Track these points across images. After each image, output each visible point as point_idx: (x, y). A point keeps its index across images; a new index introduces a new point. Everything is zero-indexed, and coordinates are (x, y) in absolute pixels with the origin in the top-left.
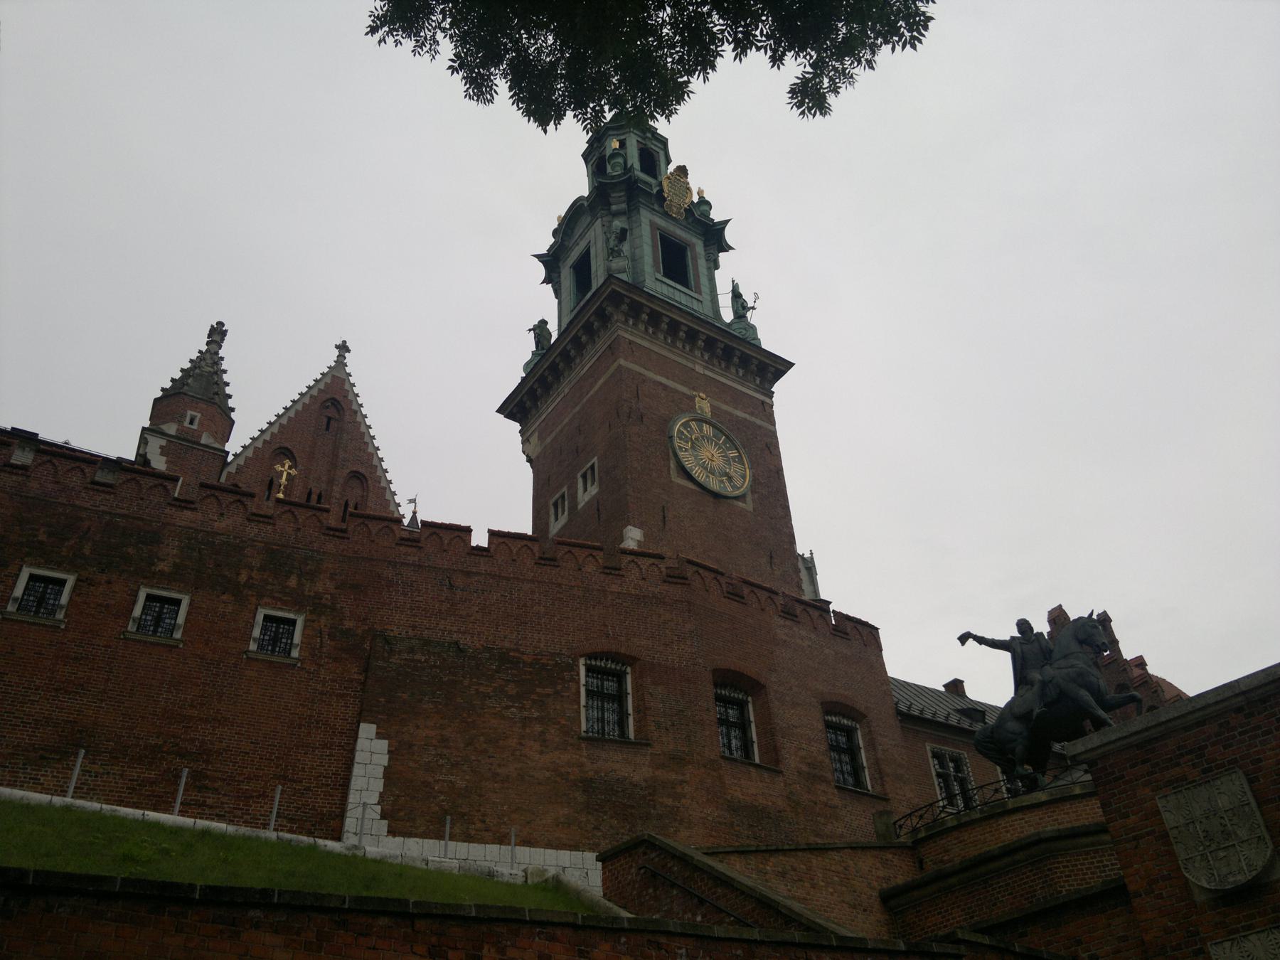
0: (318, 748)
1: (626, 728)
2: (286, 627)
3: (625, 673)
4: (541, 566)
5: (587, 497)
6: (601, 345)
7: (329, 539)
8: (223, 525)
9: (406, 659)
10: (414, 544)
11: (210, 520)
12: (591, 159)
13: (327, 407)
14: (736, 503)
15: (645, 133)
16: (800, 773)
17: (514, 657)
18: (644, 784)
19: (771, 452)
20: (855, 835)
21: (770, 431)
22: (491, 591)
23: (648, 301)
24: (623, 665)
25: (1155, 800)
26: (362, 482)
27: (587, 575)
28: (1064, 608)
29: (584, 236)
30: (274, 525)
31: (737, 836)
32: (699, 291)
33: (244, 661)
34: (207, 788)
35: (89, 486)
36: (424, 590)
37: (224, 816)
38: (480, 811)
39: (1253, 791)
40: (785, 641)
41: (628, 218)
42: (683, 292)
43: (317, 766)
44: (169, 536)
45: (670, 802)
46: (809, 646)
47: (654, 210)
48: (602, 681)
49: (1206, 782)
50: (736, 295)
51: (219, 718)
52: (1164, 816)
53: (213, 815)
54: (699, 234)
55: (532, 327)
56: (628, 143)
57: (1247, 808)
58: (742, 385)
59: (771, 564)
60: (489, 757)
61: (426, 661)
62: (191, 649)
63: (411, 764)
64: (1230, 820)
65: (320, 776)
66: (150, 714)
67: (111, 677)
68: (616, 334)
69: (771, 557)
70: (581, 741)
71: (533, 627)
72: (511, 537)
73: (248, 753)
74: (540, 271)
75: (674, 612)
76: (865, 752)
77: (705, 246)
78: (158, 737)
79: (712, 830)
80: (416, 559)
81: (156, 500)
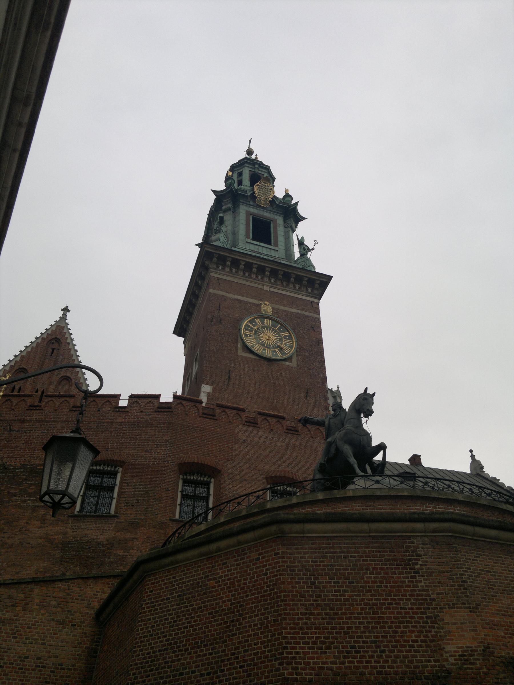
13: (53, 343)
14: (284, 363)
18: (105, 542)
19: (314, 330)
21: (316, 318)
23: (229, 254)
26: (69, 381)
32: (276, 245)
40: (244, 440)
41: (233, 212)
45: (121, 553)
46: (264, 442)
47: (250, 205)
50: (301, 243)
54: (280, 214)
59: (307, 397)
69: (307, 393)
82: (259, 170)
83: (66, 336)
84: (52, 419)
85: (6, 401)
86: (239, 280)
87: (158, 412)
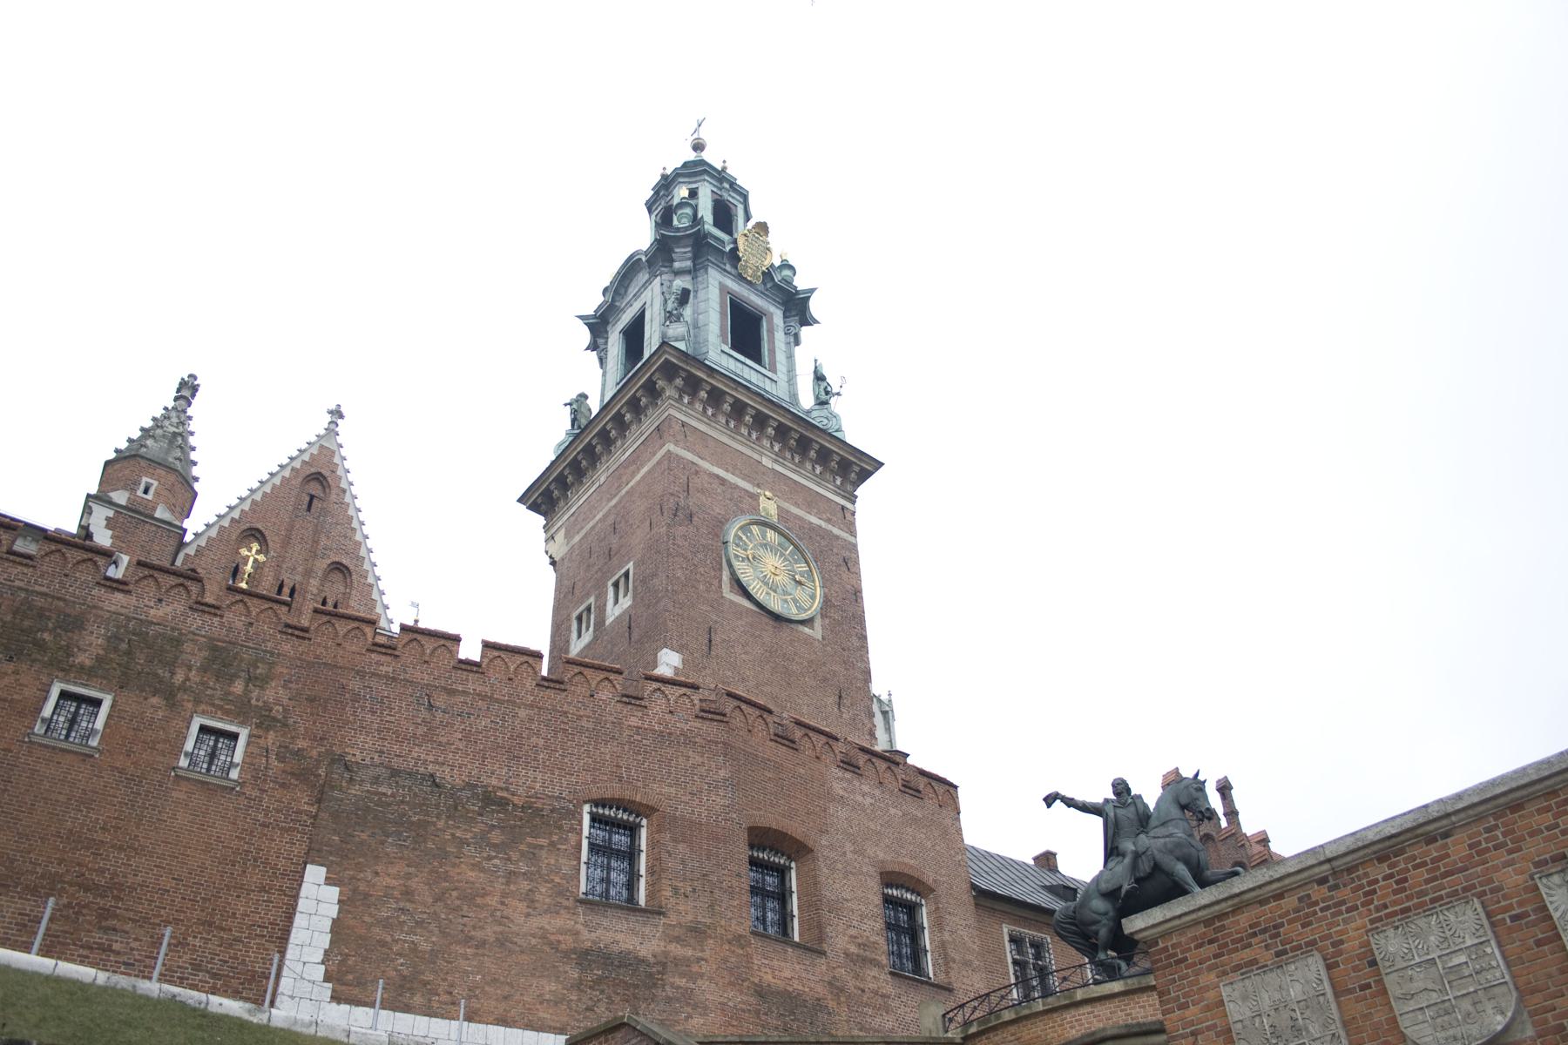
0: (254, 891)
1: (635, 893)
2: (226, 741)
3: (639, 826)
4: (544, 689)
5: (618, 611)
6: (649, 424)
7: (287, 639)
8: (160, 613)
9: (368, 791)
10: (390, 651)
11: (145, 606)
12: (656, 209)
15: (721, 183)
16: (847, 954)
17: (502, 798)
18: (652, 960)
20: (908, 1030)
21: (850, 543)
22: (478, 716)
23: (709, 376)
24: (637, 816)
25: (1219, 987)
26: (344, 575)
27: (601, 703)
28: (1180, 771)
29: (639, 296)
30: (221, 616)
31: (763, 1026)
32: (773, 369)
33: (171, 778)
34: (114, 930)
35: (5, 556)
36: (397, 708)
37: (134, 965)
38: (447, 980)
39: (1331, 979)
41: (693, 279)
42: (754, 369)
43: (252, 912)
44: (94, 622)
45: (682, 982)
46: (871, 804)
48: (610, 833)
49: (1278, 967)
50: (819, 378)
51: (136, 846)
52: (1227, 1007)
53: (119, 962)
55: (568, 401)
56: (701, 193)
57: (1321, 998)
58: (819, 484)
59: (839, 705)
60: (463, 916)
61: (393, 795)
62: (109, 760)
63: (367, 919)
64: (1302, 1014)
65: (254, 926)
66: (52, 835)
67: (8, 788)
68: (666, 414)
69: (840, 697)
70: (578, 904)
71: (528, 763)
72: (509, 651)
73: (169, 891)
74: (585, 336)
75: (706, 755)
76: (930, 933)
77: (785, 317)
78: (59, 864)
79: (732, 1018)
80: (390, 669)
81: (83, 578)
82: (730, 195)
83: (338, 473)
84: (506, 698)
85: (411, 641)
86: (718, 432)
87: (702, 718)
